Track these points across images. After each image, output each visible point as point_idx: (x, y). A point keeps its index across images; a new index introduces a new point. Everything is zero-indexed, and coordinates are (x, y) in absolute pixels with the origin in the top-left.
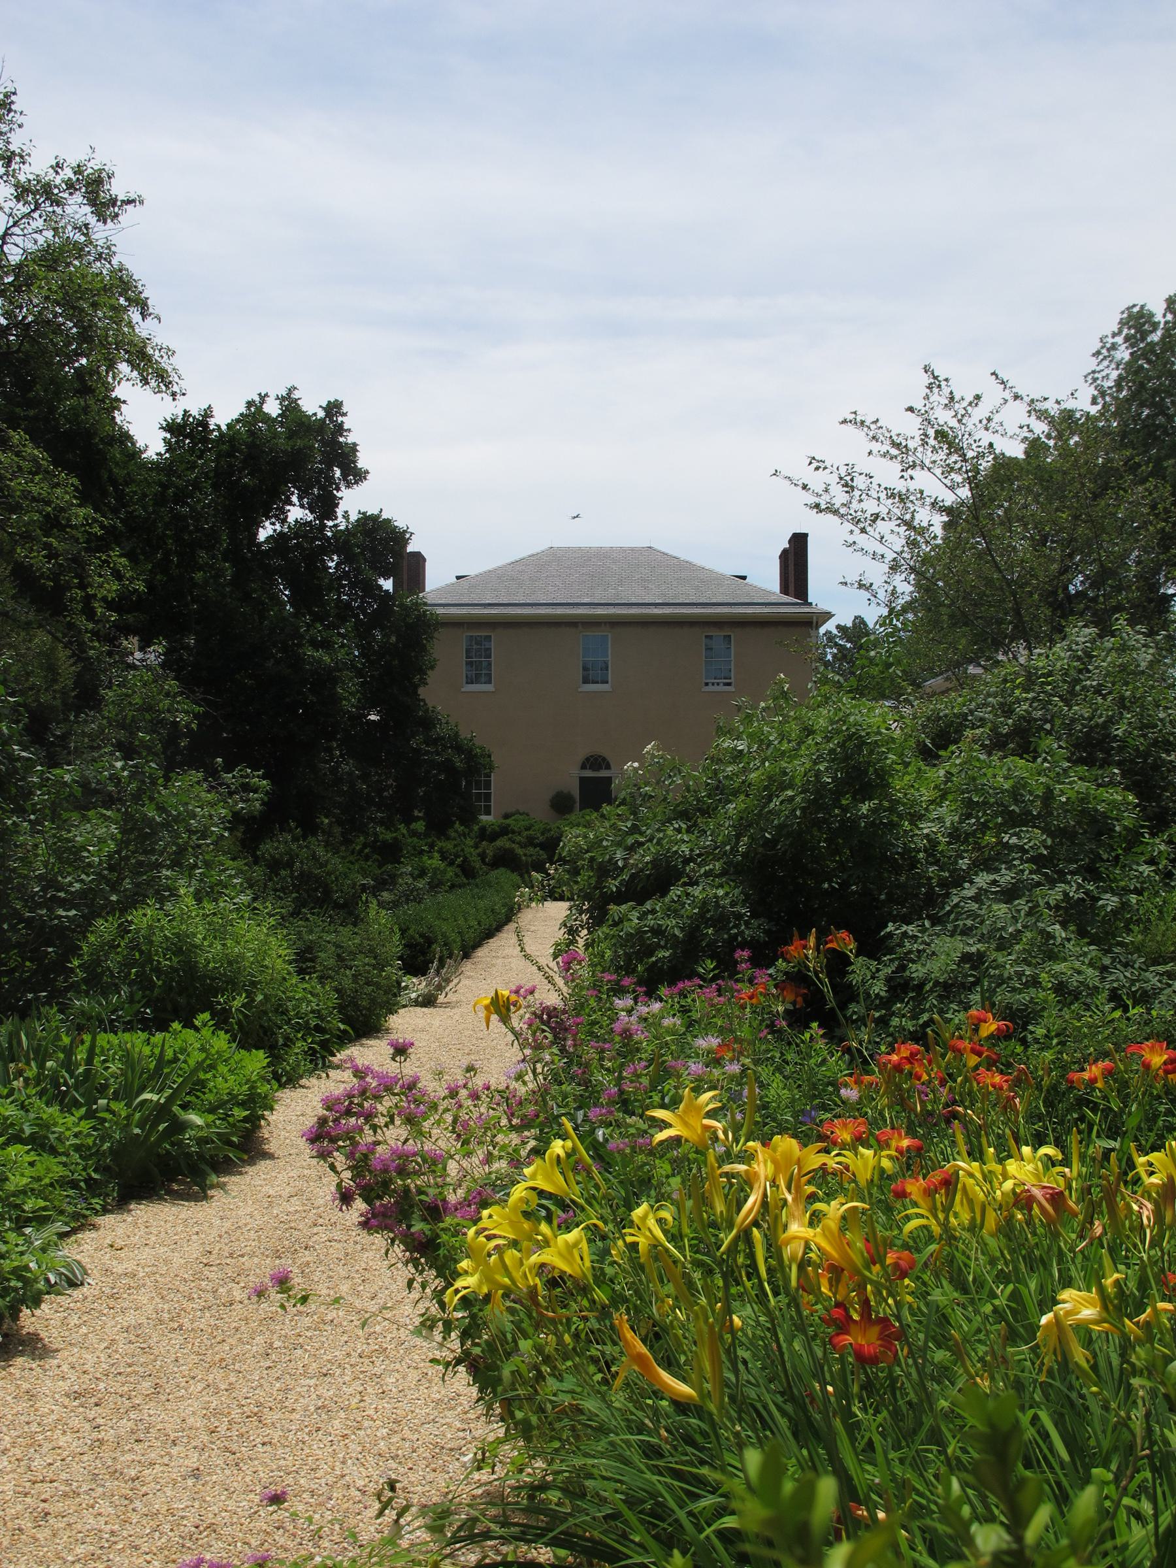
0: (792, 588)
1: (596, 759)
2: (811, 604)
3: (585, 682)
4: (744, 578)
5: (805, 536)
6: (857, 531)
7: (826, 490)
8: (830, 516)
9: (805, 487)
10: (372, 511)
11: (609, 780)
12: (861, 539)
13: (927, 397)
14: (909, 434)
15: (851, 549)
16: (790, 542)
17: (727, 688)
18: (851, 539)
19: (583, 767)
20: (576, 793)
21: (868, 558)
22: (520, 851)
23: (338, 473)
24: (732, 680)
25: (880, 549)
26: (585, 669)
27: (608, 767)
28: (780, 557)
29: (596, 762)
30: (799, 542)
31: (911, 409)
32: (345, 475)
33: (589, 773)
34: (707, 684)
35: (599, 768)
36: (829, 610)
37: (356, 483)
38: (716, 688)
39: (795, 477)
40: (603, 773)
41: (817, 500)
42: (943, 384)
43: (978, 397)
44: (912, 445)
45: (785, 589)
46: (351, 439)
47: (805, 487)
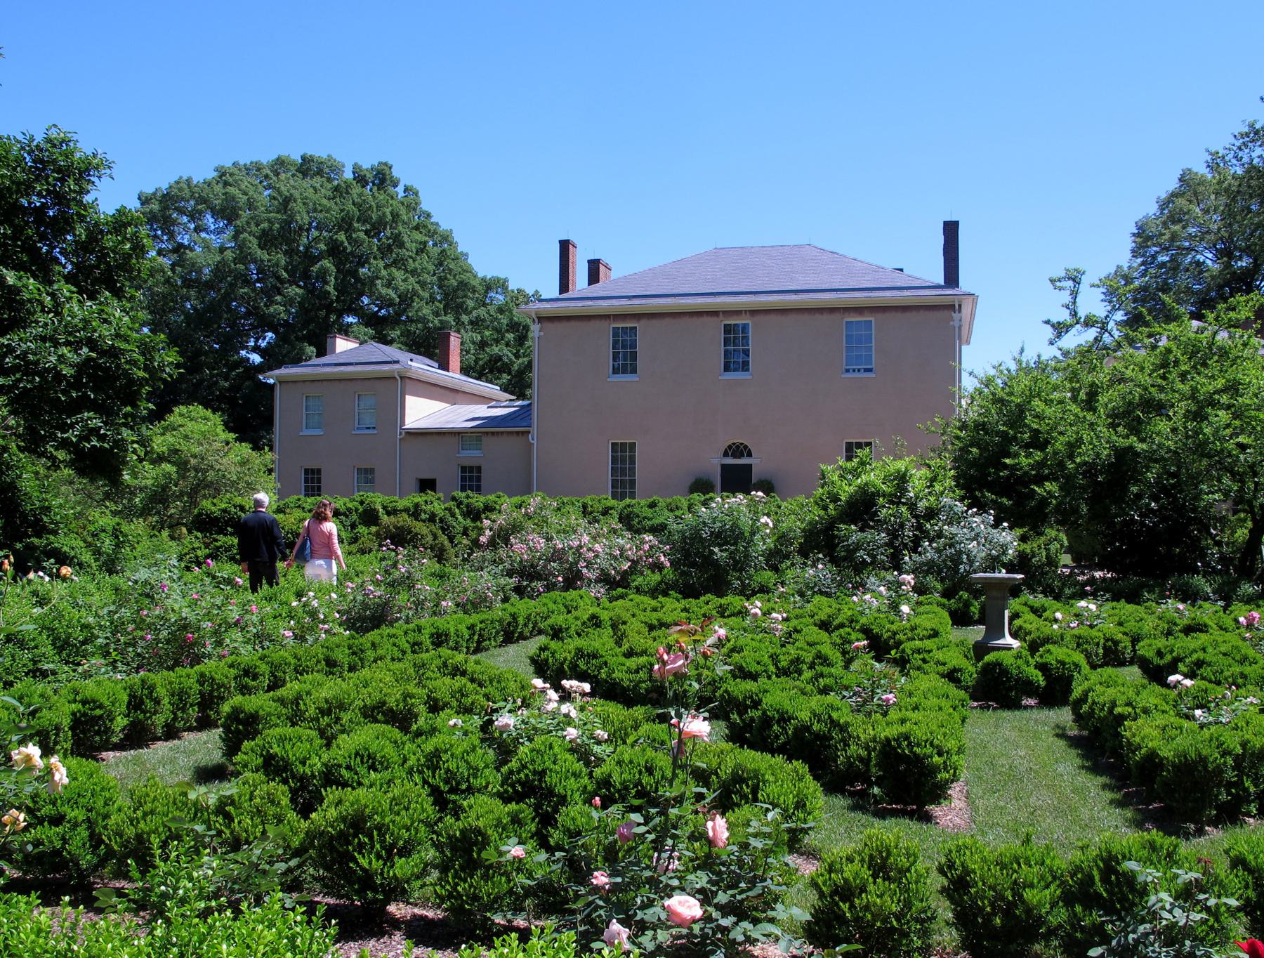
1: (738, 447)
4: (902, 270)
5: (956, 223)
19: (726, 454)
24: (873, 366)
27: (750, 455)
29: (738, 450)
30: (951, 229)
34: (848, 371)
35: (741, 455)
36: (972, 292)
38: (856, 375)
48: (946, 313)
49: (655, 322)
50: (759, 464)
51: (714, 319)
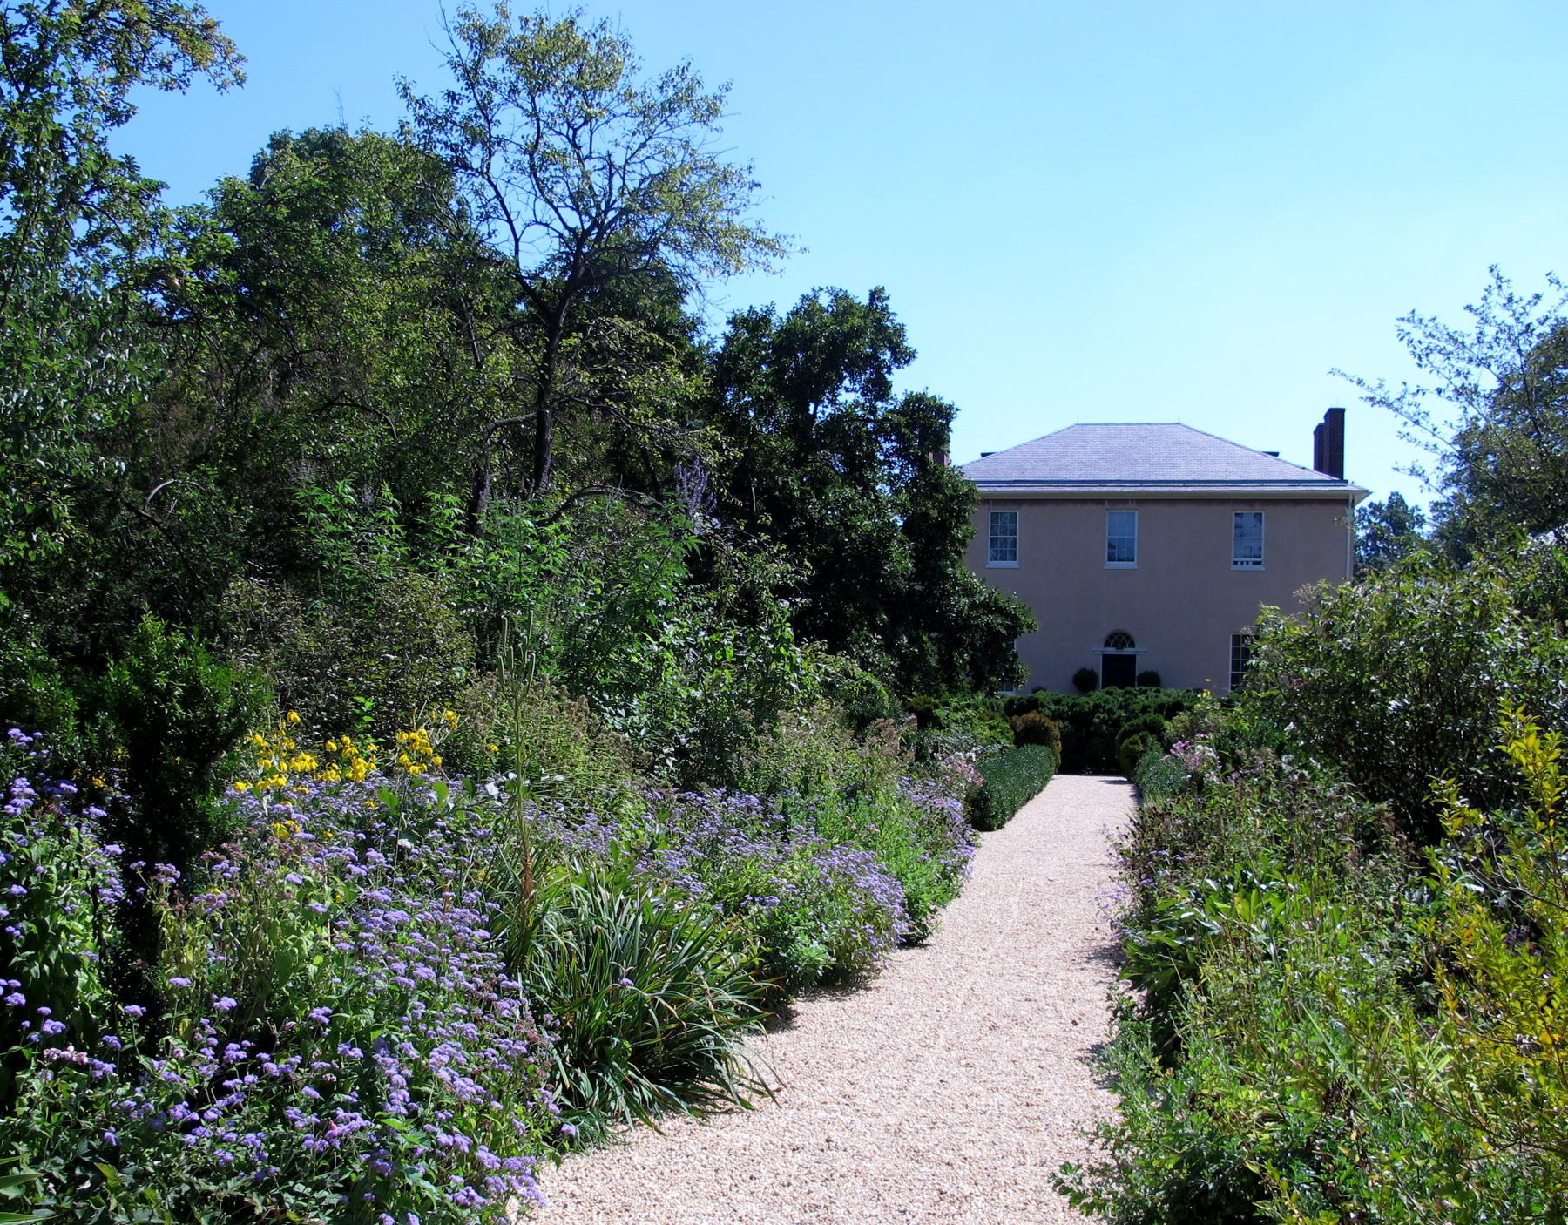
0: (1326, 464)
2: (1347, 482)
3: (1111, 559)
4: (1276, 454)
6: (1410, 423)
7: (1381, 386)
8: (1384, 409)
9: (1360, 382)
10: (917, 389)
11: (1132, 659)
12: (1414, 431)
13: (1485, 298)
14: (1466, 332)
15: (1405, 440)
16: (1326, 417)
17: (1257, 567)
18: (1404, 430)
19: (1107, 645)
20: (1099, 671)
21: (1421, 449)
22: (1049, 724)
23: (888, 356)
25: (1433, 441)
26: (1111, 546)
27: (1132, 644)
28: (1315, 432)
29: (1119, 639)
30: (1335, 419)
31: (1469, 308)
32: (896, 360)
33: (1111, 651)
34: (1236, 563)
35: (1124, 645)
36: (1366, 487)
37: (907, 362)
38: (1245, 567)
39: (1349, 374)
40: (1127, 651)
41: (1371, 395)
42: (1504, 286)
43: (1538, 297)
44: (1468, 342)
45: (1319, 466)
46: (898, 320)
47: (1360, 382)
48: (1339, 508)
49: (1037, 509)
50: (1145, 657)
51: (1099, 508)
